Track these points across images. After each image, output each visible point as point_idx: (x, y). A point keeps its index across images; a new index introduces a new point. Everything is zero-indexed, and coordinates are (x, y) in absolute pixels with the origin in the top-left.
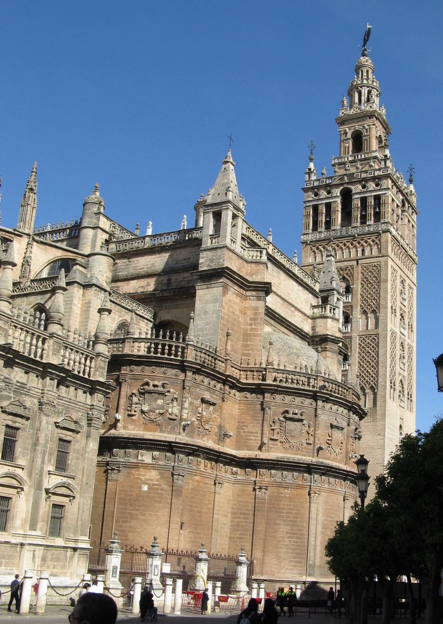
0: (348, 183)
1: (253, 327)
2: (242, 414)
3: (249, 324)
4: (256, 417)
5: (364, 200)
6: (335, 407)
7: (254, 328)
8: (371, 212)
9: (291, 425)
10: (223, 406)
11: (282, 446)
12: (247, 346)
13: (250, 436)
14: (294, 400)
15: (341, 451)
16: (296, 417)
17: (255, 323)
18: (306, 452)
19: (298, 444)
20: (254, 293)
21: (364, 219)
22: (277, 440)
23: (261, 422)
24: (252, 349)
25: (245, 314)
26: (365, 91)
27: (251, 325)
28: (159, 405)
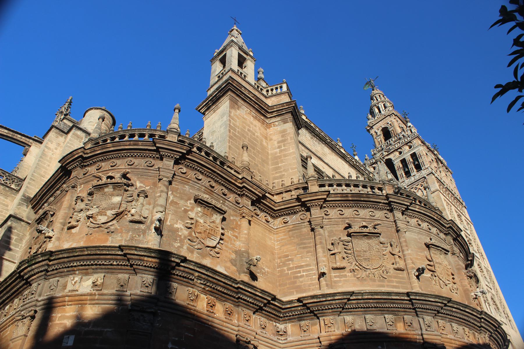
0: (387, 155)
1: (283, 148)
2: (283, 246)
3: (277, 146)
4: (305, 244)
5: (403, 161)
6: (425, 225)
7: (285, 149)
8: (411, 166)
9: (361, 244)
10: (242, 225)
11: (355, 276)
12: (279, 168)
13: (300, 272)
14: (357, 213)
15: (455, 286)
16: (365, 230)
17: (283, 144)
18: (397, 282)
19: (381, 271)
20: (279, 119)
21: (408, 174)
22: (343, 268)
23: (313, 249)
24: (284, 170)
25: (271, 140)
26: (381, 105)
27: (279, 147)
28: (114, 204)
